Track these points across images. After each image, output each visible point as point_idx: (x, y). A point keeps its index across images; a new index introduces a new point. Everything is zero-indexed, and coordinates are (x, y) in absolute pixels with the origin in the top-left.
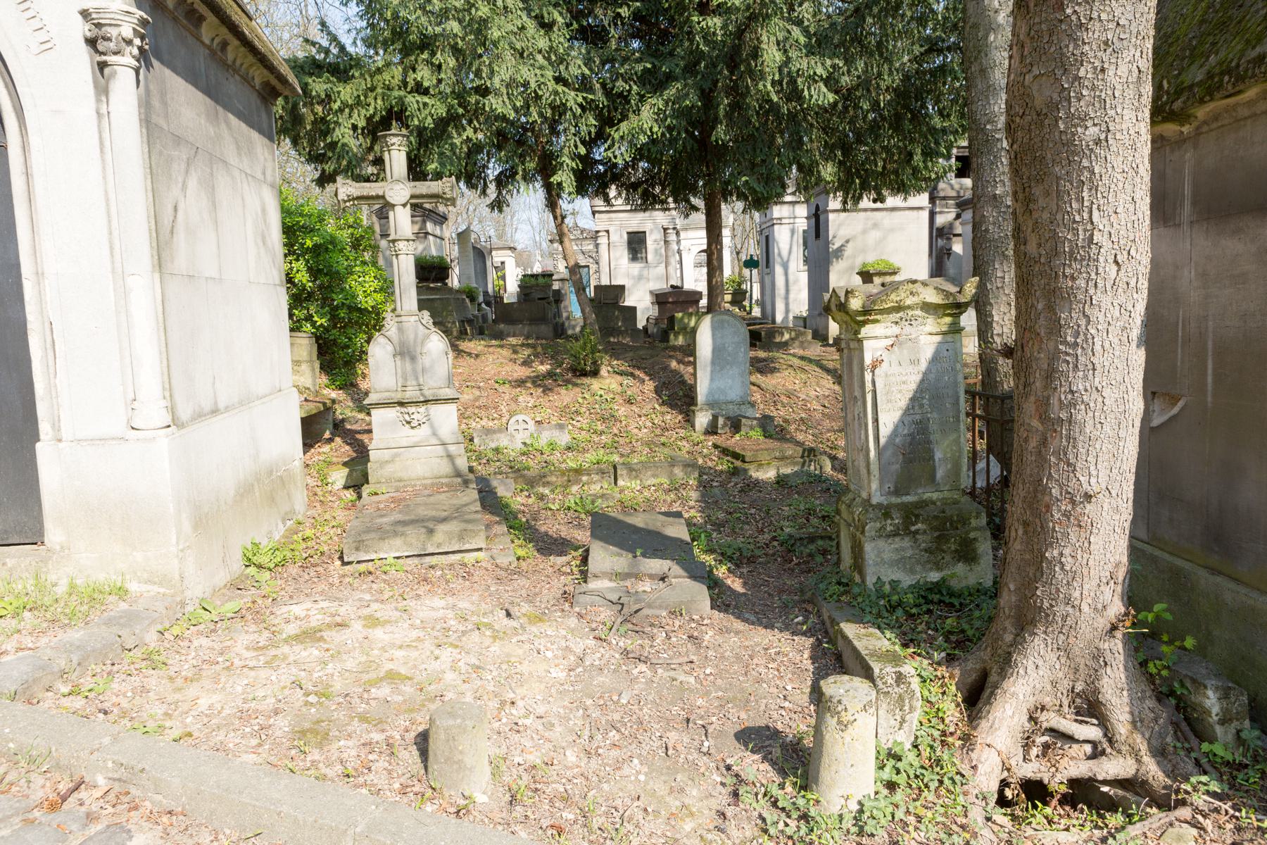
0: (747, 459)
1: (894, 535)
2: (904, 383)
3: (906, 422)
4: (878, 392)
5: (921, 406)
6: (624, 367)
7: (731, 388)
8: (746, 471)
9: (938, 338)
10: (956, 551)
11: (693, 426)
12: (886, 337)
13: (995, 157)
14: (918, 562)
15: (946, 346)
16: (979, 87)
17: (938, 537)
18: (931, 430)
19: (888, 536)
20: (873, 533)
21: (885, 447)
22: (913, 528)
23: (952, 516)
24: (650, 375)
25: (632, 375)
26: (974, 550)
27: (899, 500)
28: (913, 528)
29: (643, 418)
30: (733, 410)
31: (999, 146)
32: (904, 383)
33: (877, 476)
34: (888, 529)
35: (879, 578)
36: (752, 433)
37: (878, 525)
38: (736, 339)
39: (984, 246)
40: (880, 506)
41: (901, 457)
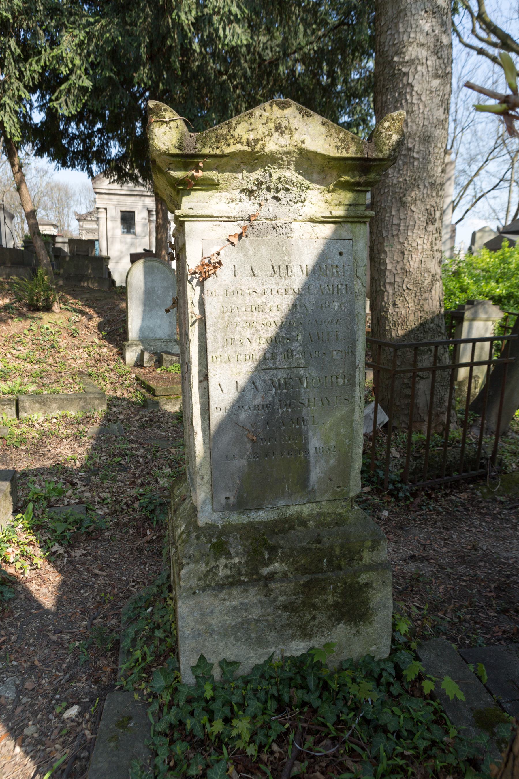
0: (157, 393)
1: (232, 585)
2: (258, 308)
3: (259, 383)
4: (209, 322)
5: (289, 354)
6: (79, 306)
7: (160, 327)
8: (157, 403)
9: (327, 230)
10: (336, 605)
11: (124, 359)
12: (230, 219)
13: (400, 93)
14: (271, 627)
15: (339, 246)
16: (390, 13)
17: (306, 585)
18: (304, 398)
19: (220, 587)
20: (194, 582)
21: (223, 425)
22: (265, 571)
23: (332, 548)
24: (98, 313)
25: (82, 313)
26: (365, 602)
27: (244, 519)
28: (265, 571)
29: (81, 350)
30: (160, 346)
31: (405, 81)
32: (258, 308)
33: (207, 478)
34: (222, 573)
35: (202, 658)
36: (171, 368)
37: (203, 568)
38: (165, 284)
39: (382, 192)
40: (211, 527)
41: (249, 446)
